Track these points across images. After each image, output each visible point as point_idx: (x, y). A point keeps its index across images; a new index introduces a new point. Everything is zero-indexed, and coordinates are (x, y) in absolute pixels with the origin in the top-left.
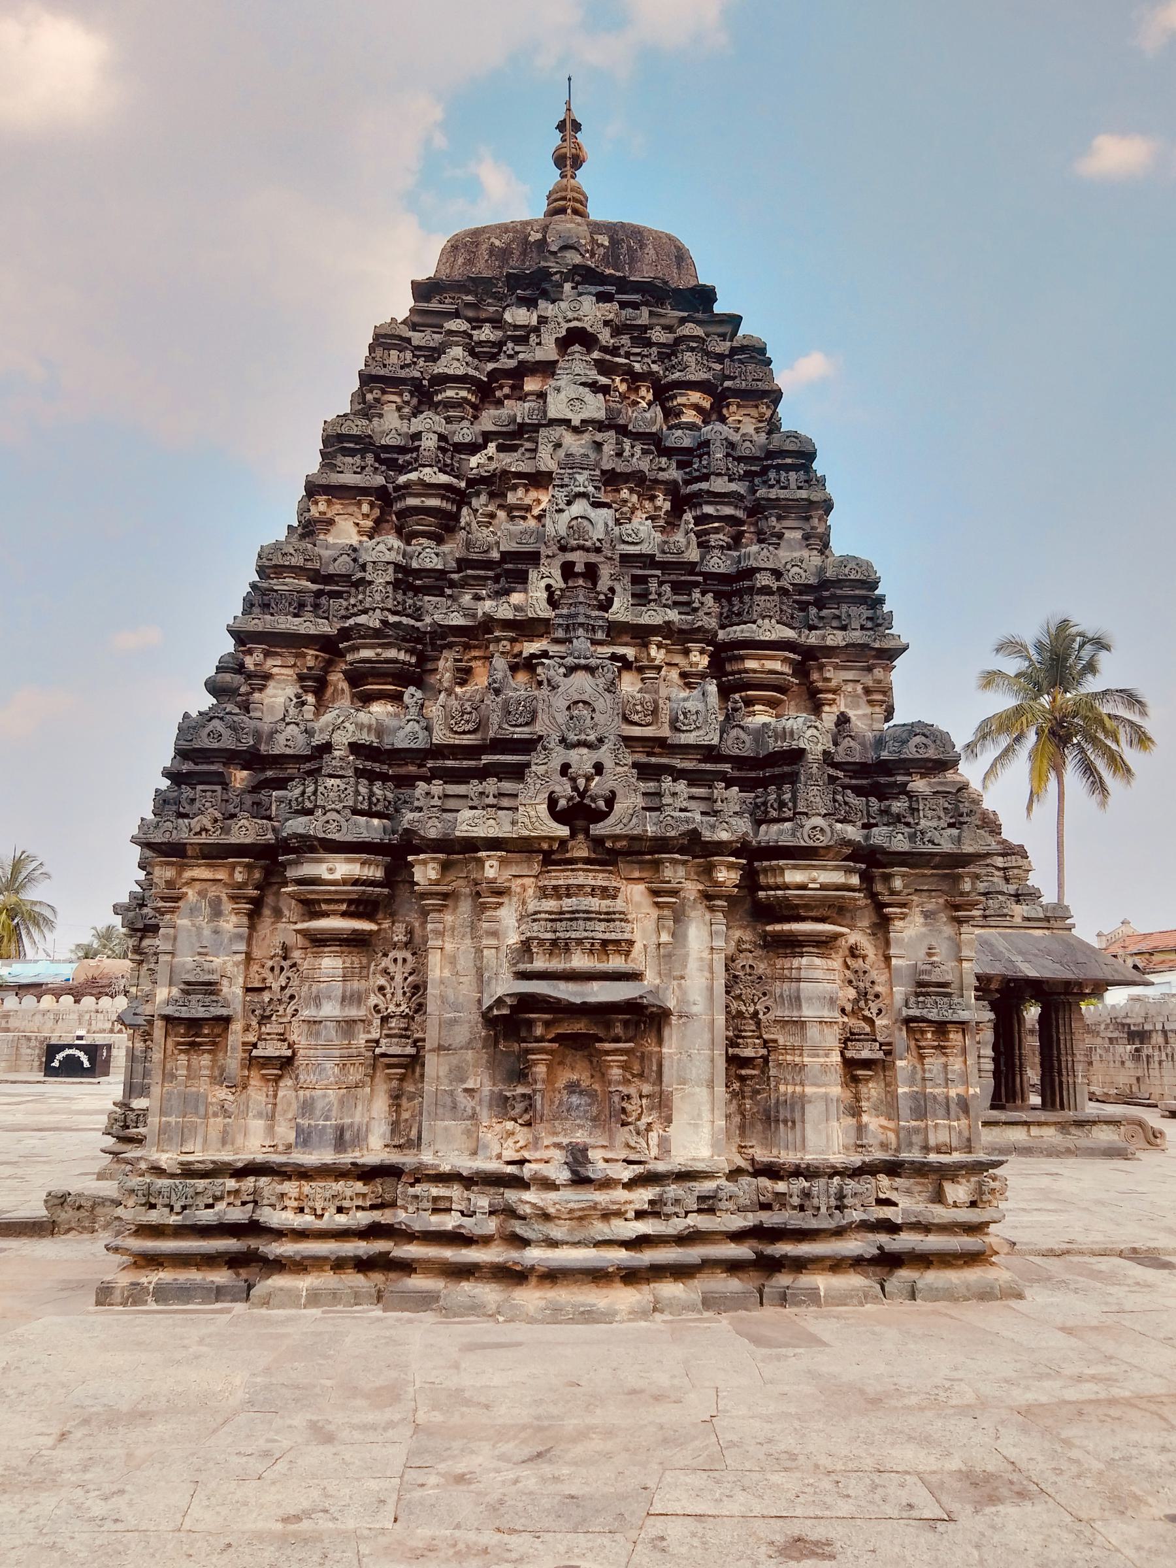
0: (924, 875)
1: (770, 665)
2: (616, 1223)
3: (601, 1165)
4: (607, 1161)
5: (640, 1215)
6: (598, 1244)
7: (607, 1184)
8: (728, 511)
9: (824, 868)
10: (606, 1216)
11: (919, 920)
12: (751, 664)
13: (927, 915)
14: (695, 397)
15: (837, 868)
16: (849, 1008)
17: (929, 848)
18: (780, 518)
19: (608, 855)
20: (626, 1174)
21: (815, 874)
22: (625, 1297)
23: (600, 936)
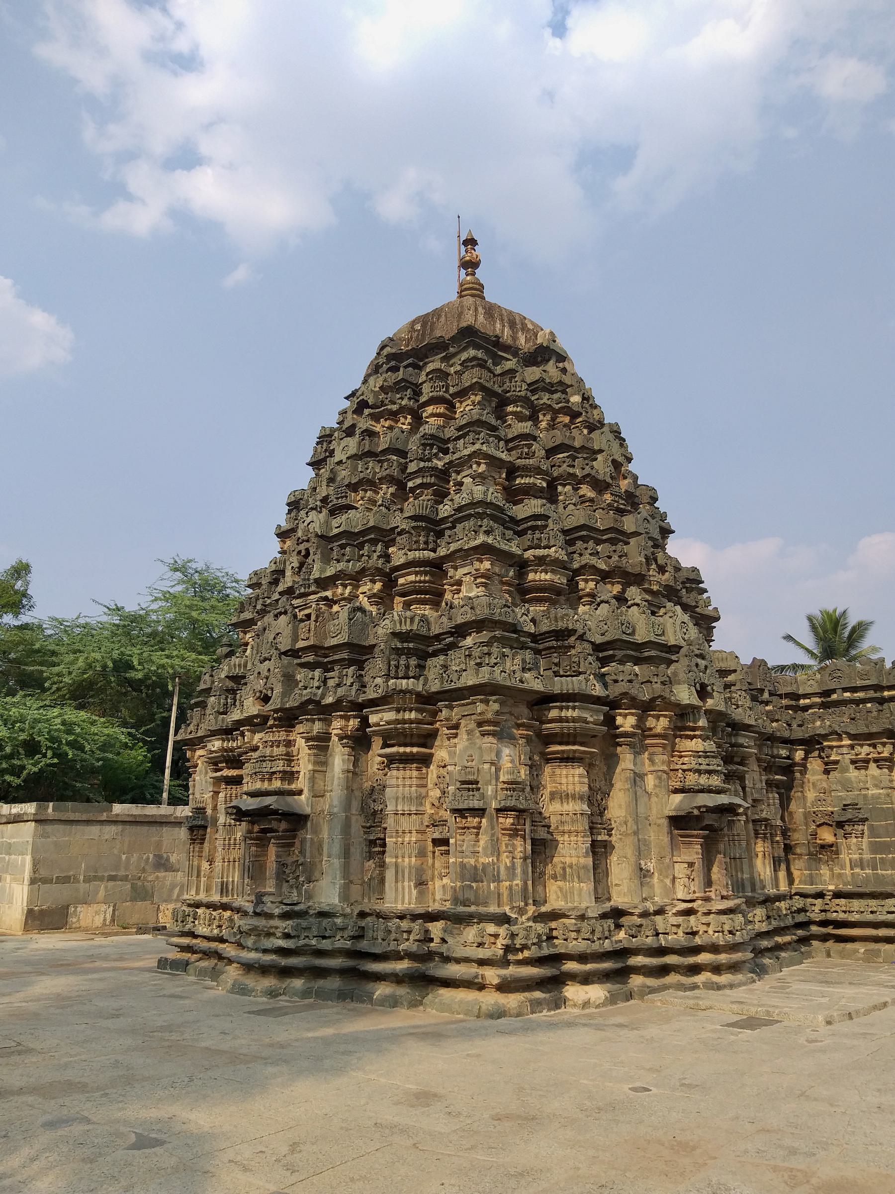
0: (463, 705)
1: (412, 578)
2: (272, 939)
3: (269, 904)
4: (272, 902)
5: (287, 936)
6: (265, 951)
7: (269, 916)
8: (419, 481)
9: (383, 711)
10: (269, 935)
11: (465, 737)
12: (401, 581)
13: (469, 733)
14: (430, 409)
15: (390, 710)
16: (437, 804)
17: (453, 686)
18: (458, 473)
19: (288, 719)
20: (277, 911)
21: (380, 715)
22: (269, 982)
23: (268, 769)
